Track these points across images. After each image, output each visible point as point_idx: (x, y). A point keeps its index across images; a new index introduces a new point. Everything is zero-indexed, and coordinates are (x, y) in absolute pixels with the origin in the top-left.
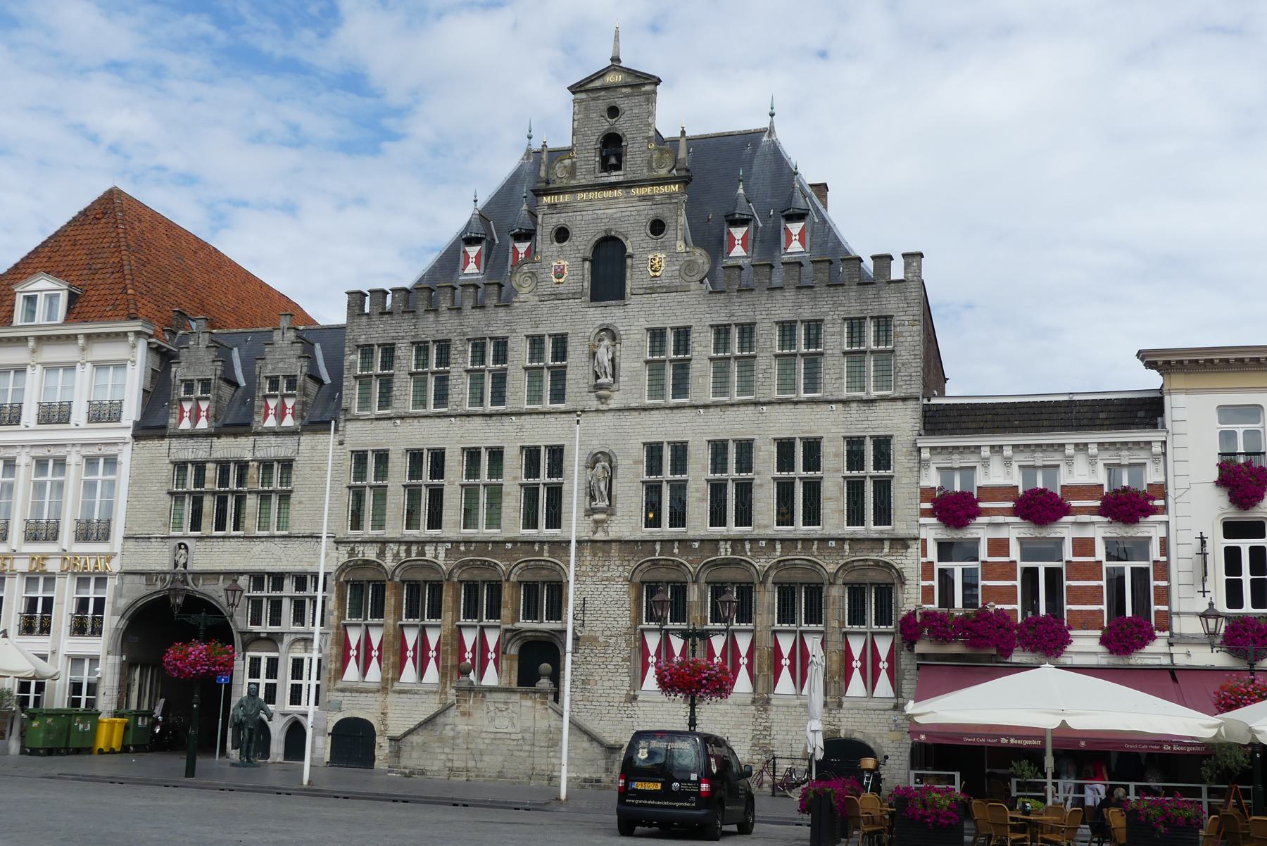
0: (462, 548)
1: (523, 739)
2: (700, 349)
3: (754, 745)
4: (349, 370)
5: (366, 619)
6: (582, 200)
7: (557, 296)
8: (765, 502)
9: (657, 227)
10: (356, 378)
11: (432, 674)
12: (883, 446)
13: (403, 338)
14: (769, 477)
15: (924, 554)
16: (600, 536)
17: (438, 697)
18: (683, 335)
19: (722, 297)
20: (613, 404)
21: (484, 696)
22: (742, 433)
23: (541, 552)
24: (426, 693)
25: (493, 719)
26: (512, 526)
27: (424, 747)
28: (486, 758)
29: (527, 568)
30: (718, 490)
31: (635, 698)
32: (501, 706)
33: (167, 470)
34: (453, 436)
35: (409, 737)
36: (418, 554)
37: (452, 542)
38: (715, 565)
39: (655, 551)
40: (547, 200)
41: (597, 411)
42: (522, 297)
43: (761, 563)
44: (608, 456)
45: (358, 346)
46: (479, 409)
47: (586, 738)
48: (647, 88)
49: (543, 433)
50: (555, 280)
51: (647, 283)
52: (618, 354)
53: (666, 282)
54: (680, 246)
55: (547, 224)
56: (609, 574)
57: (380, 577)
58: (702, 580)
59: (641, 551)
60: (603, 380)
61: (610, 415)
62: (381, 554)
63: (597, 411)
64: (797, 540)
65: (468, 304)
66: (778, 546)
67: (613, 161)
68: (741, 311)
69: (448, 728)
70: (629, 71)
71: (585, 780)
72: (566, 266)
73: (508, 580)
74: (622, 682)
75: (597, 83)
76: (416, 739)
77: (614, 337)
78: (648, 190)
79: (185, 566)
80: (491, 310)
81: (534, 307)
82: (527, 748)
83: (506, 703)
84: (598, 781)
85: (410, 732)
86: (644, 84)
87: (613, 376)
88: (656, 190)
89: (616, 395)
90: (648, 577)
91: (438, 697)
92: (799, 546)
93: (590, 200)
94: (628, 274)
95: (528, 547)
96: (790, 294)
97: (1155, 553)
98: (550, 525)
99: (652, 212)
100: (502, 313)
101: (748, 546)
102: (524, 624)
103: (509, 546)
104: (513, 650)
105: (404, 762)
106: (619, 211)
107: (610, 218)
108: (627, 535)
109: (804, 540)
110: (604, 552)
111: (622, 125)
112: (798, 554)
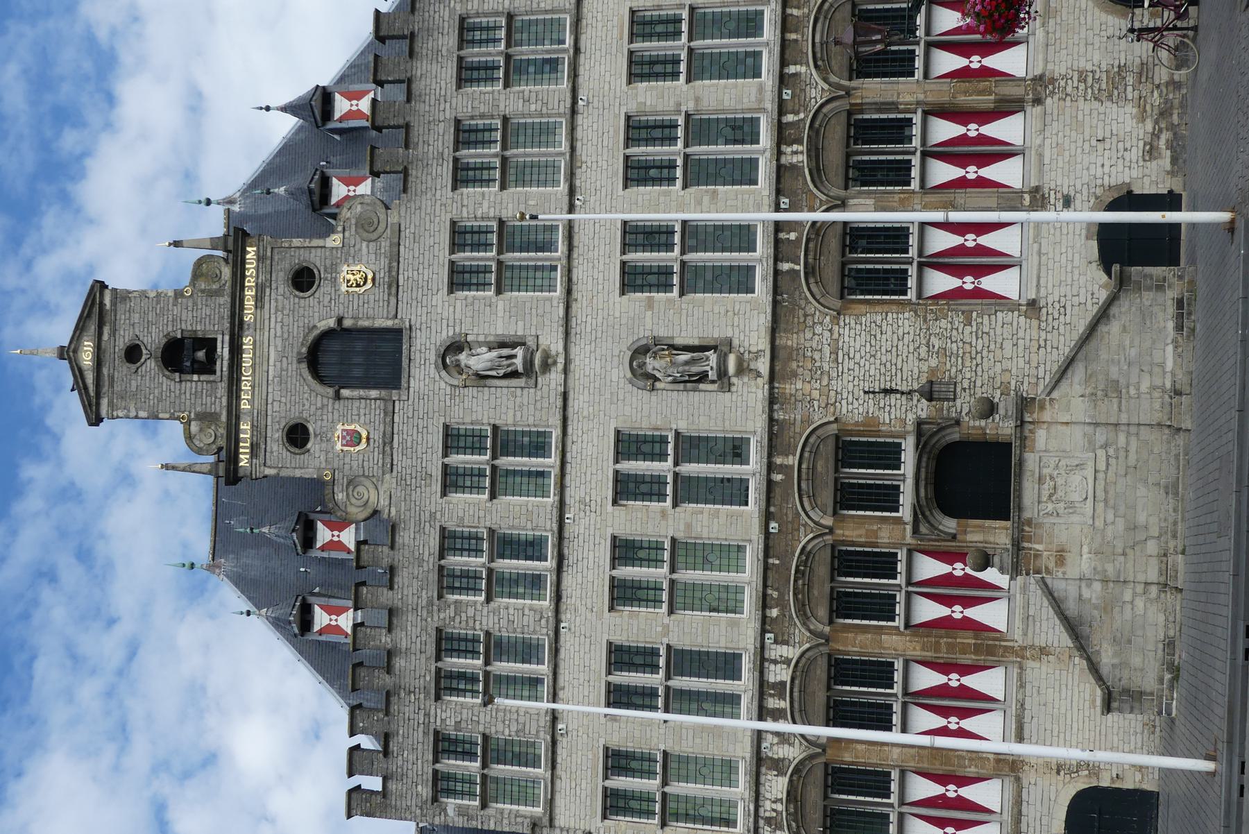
0: (774, 613)
1: (1105, 446)
2: (486, 204)
3: (1110, 97)
4: (470, 818)
5: (891, 805)
6: (251, 402)
7: (388, 440)
9: (303, 279)
10: (484, 806)
11: (988, 682)
13: (427, 715)
14: (685, 87)
16: (763, 366)
17: (1030, 664)
19: (413, 172)
20: (557, 347)
21: (1029, 522)
22: (617, 132)
23: (785, 469)
24: (1022, 686)
25: (1071, 505)
26: (742, 523)
27: (1122, 642)
28: (1142, 518)
29: (813, 497)
31: (1032, 304)
32: (1048, 485)
34: (591, 626)
35: (1105, 671)
36: (781, 696)
37: (763, 631)
38: (817, 172)
39: (792, 271)
40: (244, 460)
41: (566, 371)
42: (384, 502)
43: (817, 91)
44: (640, 351)
45: (435, 799)
46: (550, 579)
47: (1102, 328)
48: (107, 300)
49: (593, 465)
50: (363, 445)
51: (381, 293)
52: (481, 338)
53: (384, 262)
54: (335, 240)
55: (281, 460)
56: (827, 350)
57: (819, 773)
58: (842, 193)
59: (791, 295)
60: (519, 363)
61: (574, 350)
62: (778, 765)
63: (566, 371)
64: (783, 40)
65: (385, 596)
66: (792, 69)
67: (201, 355)
68: (436, 142)
69: (1086, 594)
70: (80, 329)
71: (1179, 328)
72: (345, 429)
73: (831, 531)
74: (1001, 323)
75: (90, 378)
76: (1107, 658)
77: (456, 347)
78: (250, 293)
80: (399, 557)
81: (401, 480)
82: (1122, 439)
83: (1041, 480)
84: (1180, 303)
85: (1094, 668)
86: (102, 304)
87: (513, 346)
88: (250, 282)
89: (544, 342)
90: (834, 287)
91: (1030, 664)
92: (793, 36)
93: (253, 387)
94: (365, 323)
95: (778, 491)
96: (421, 67)
99: (281, 287)
100: (404, 537)
101: (790, 118)
102: (905, 511)
103: (774, 525)
104: (950, 524)
105: (1149, 682)
106: (273, 338)
107: (282, 356)
108: (763, 319)
109: (785, 29)
110: (790, 358)
111: (153, 340)
112: (805, 38)
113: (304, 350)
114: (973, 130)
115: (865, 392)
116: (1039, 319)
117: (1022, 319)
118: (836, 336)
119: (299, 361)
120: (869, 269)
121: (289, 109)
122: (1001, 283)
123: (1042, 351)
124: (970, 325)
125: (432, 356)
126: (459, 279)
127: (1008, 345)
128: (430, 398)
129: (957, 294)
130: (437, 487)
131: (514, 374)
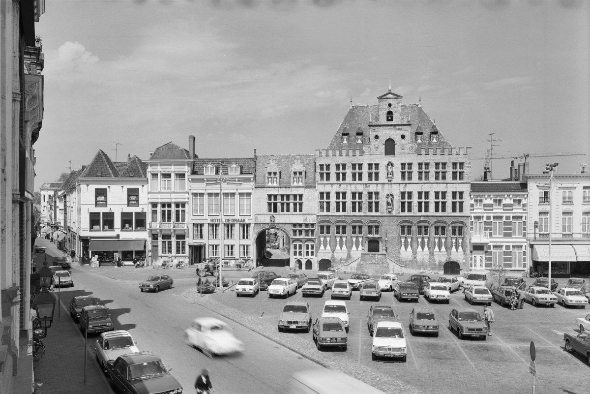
8: (432, 207)
9: (403, 137)
12: (461, 194)
15: (471, 219)
18: (410, 165)
30: (420, 204)
33: (267, 197)
44: (392, 195)
49: (373, 189)
67: (390, 118)
79: (274, 221)
89: (393, 180)
97: (524, 219)
98: (376, 211)
111: (391, 109)
114: (426, 244)
119: (390, 137)
120: (405, 229)
126: (403, 165)
128: (383, 161)
130: (369, 162)
131: (388, 175)
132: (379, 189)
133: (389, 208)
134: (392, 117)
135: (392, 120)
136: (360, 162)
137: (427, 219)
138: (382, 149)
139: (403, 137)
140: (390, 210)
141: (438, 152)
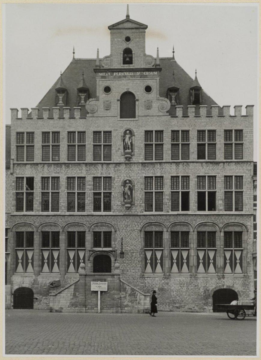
9: (148, 89)
40: (101, 74)
77: (131, 133)
87: (132, 149)
113: (130, 90)
115: (122, 238)
116: (140, 278)
117: (140, 274)
118: (136, 230)
120: (152, 239)
121: (196, 78)
122: (149, 269)
123: (133, 279)
124: (138, 262)
125: (129, 127)
126: (148, 133)
127: (134, 271)
129: (146, 258)
130: (96, 130)
132: (111, 172)
133: (126, 203)
134: (131, 58)
135: (130, 62)
136: (29, 130)
137: (159, 220)
138: (116, 107)
139: (148, 89)
140: (129, 205)
141: (65, 116)
